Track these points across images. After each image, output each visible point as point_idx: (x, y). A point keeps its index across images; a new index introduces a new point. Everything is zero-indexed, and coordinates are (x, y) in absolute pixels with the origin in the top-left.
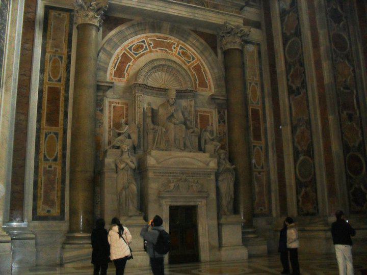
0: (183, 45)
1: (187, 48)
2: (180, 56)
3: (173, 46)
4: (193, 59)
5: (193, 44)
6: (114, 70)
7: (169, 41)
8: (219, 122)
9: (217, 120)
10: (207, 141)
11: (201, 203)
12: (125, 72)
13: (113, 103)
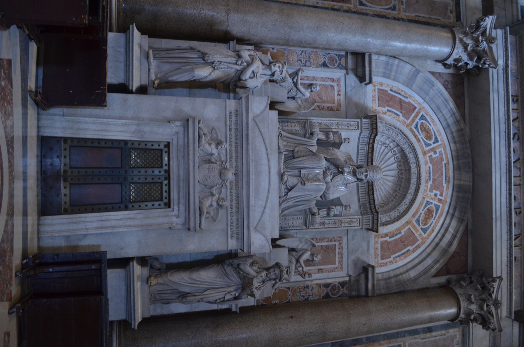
1: (439, 218)
2: (425, 206)
3: (438, 193)
4: (424, 230)
5: (447, 230)
6: (388, 89)
7: (445, 185)
8: (327, 286)
10: (294, 253)
11: (175, 216)
12: (387, 108)
13: (338, 85)
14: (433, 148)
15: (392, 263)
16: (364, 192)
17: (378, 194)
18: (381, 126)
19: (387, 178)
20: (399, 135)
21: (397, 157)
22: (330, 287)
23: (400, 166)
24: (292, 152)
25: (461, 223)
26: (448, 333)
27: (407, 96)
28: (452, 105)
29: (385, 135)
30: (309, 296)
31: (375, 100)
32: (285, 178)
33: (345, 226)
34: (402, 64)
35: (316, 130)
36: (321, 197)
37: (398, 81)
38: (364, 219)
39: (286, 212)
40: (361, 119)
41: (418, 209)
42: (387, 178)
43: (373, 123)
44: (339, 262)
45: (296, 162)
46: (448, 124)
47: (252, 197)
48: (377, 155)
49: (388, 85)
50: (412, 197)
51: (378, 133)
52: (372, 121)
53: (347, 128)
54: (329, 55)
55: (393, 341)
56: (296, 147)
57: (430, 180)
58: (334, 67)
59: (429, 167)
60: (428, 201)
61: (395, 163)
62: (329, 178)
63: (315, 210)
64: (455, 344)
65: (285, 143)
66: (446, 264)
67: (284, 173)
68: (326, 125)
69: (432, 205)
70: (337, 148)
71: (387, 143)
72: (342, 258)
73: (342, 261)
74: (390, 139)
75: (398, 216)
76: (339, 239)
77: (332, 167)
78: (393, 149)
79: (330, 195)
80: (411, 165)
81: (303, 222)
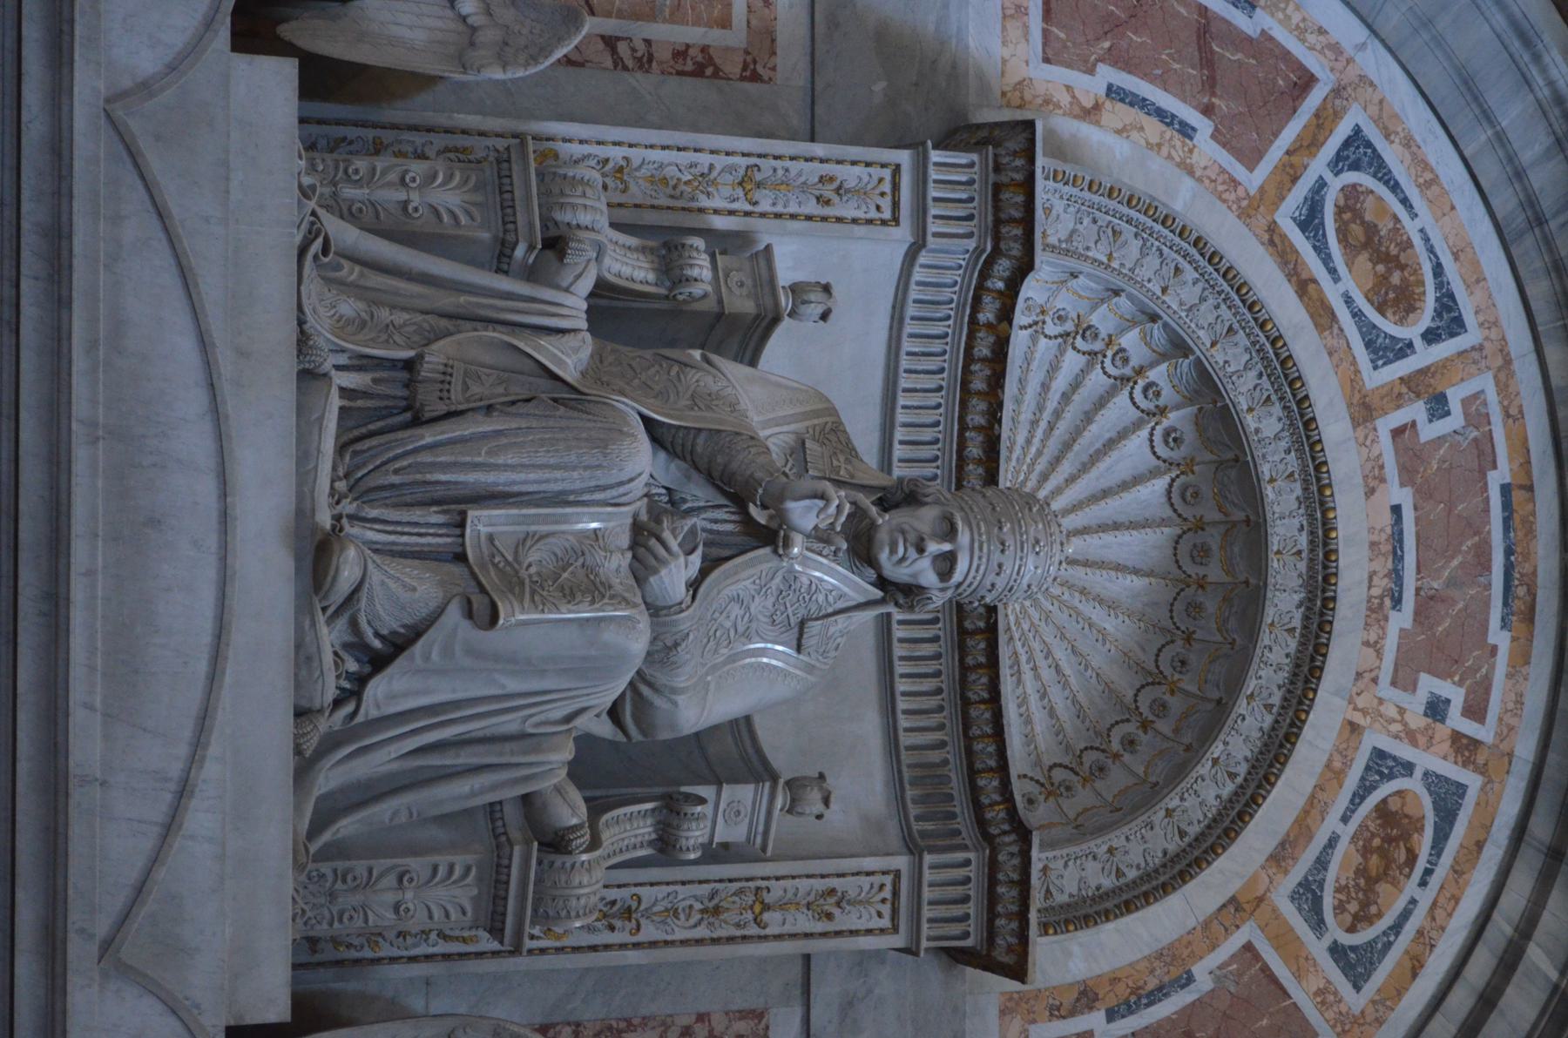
0: (1487, 810)
1: (1458, 871)
3: (1456, 695)
4: (1354, 963)
7: (1500, 638)
12: (1107, 74)
14: (1423, 372)
16: (928, 685)
17: (1033, 699)
18: (1059, 205)
19: (1099, 581)
20: (1190, 274)
21: (1167, 433)
23: (1190, 495)
24: (404, 375)
29: (1086, 267)
32: (348, 567)
33: (787, 929)
35: (584, 218)
36: (614, 713)
38: (928, 876)
39: (347, 826)
40: (916, 145)
41: (1314, 806)
42: (1099, 581)
43: (1004, 179)
45: (431, 447)
46: (1530, 202)
47: (89, 707)
48: (1026, 416)
50: (1269, 720)
51: (1040, 256)
52: (998, 169)
53: (811, 207)
56: (429, 343)
57: (1397, 602)
60: (1379, 754)
61: (1153, 474)
62: (675, 576)
63: (570, 811)
65: (349, 307)
67: (337, 529)
68: (665, 181)
69: (1414, 784)
70: (738, 358)
71: (1103, 334)
74: (1122, 301)
75: (1171, 860)
77: (698, 493)
78: (1140, 371)
79: (681, 699)
80: (1269, 492)
81: (476, 900)
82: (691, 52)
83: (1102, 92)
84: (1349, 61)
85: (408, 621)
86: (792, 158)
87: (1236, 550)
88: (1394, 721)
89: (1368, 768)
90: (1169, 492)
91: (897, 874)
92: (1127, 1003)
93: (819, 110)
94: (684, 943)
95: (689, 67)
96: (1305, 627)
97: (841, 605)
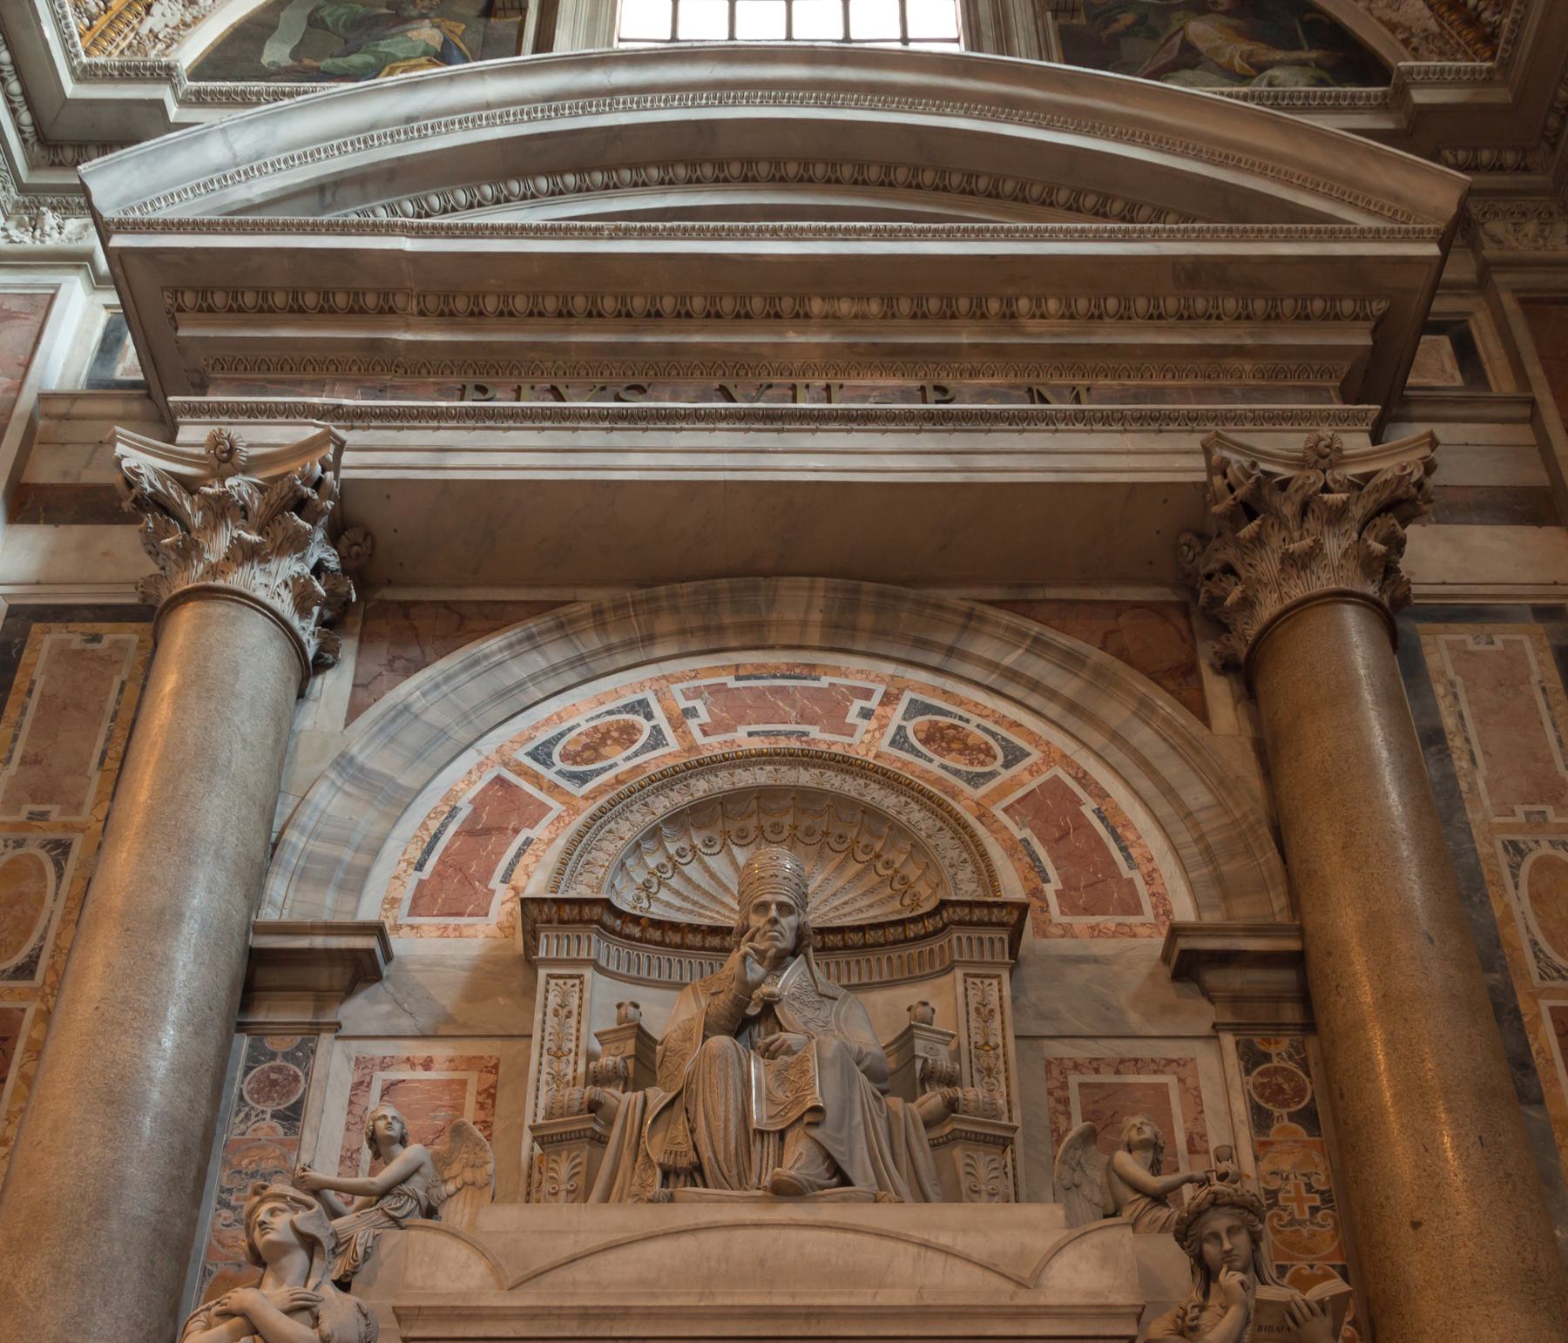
0: (923, 688)
1: (961, 702)
3: (857, 705)
4: (1014, 756)
5: (1012, 675)
6: (413, 879)
7: (825, 682)
9: (1240, 1108)
12: (495, 882)
13: (384, 1065)
14: (670, 720)
15: (1155, 875)
21: (707, 846)
22: (1269, 1106)
25: (982, 619)
26: (1443, 673)
27: (447, 809)
28: (492, 642)
30: (1309, 1188)
31: (457, 928)
34: (307, 818)
37: (383, 839)
44: (1155, 1072)
46: (571, 664)
49: (397, 878)
53: (573, 1021)
54: (246, 1097)
55: (1491, 871)
57: (804, 734)
58: (300, 1074)
59: (750, 734)
60: (893, 743)
61: (730, 854)
64: (1490, 647)
66: (1155, 677)
71: (648, 877)
72: (1136, 1060)
73: (1153, 1061)
76: (1055, 1072)
78: (670, 858)
82: (481, 1100)
83: (505, 886)
84: (487, 758)
85: (820, 1160)
86: (543, 1031)
87: (774, 806)
88: (873, 736)
89: (901, 749)
90: (740, 846)
91: (966, 975)
92: (1039, 872)
93: (516, 1032)
94: (1008, 1087)
95: (490, 1101)
96: (819, 767)
97: (808, 975)
